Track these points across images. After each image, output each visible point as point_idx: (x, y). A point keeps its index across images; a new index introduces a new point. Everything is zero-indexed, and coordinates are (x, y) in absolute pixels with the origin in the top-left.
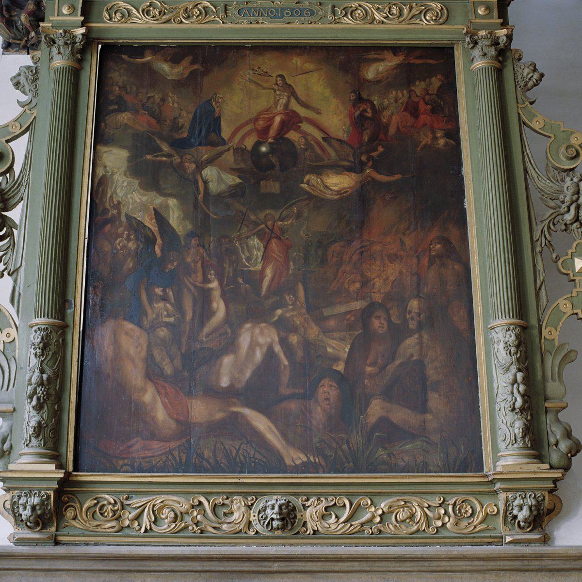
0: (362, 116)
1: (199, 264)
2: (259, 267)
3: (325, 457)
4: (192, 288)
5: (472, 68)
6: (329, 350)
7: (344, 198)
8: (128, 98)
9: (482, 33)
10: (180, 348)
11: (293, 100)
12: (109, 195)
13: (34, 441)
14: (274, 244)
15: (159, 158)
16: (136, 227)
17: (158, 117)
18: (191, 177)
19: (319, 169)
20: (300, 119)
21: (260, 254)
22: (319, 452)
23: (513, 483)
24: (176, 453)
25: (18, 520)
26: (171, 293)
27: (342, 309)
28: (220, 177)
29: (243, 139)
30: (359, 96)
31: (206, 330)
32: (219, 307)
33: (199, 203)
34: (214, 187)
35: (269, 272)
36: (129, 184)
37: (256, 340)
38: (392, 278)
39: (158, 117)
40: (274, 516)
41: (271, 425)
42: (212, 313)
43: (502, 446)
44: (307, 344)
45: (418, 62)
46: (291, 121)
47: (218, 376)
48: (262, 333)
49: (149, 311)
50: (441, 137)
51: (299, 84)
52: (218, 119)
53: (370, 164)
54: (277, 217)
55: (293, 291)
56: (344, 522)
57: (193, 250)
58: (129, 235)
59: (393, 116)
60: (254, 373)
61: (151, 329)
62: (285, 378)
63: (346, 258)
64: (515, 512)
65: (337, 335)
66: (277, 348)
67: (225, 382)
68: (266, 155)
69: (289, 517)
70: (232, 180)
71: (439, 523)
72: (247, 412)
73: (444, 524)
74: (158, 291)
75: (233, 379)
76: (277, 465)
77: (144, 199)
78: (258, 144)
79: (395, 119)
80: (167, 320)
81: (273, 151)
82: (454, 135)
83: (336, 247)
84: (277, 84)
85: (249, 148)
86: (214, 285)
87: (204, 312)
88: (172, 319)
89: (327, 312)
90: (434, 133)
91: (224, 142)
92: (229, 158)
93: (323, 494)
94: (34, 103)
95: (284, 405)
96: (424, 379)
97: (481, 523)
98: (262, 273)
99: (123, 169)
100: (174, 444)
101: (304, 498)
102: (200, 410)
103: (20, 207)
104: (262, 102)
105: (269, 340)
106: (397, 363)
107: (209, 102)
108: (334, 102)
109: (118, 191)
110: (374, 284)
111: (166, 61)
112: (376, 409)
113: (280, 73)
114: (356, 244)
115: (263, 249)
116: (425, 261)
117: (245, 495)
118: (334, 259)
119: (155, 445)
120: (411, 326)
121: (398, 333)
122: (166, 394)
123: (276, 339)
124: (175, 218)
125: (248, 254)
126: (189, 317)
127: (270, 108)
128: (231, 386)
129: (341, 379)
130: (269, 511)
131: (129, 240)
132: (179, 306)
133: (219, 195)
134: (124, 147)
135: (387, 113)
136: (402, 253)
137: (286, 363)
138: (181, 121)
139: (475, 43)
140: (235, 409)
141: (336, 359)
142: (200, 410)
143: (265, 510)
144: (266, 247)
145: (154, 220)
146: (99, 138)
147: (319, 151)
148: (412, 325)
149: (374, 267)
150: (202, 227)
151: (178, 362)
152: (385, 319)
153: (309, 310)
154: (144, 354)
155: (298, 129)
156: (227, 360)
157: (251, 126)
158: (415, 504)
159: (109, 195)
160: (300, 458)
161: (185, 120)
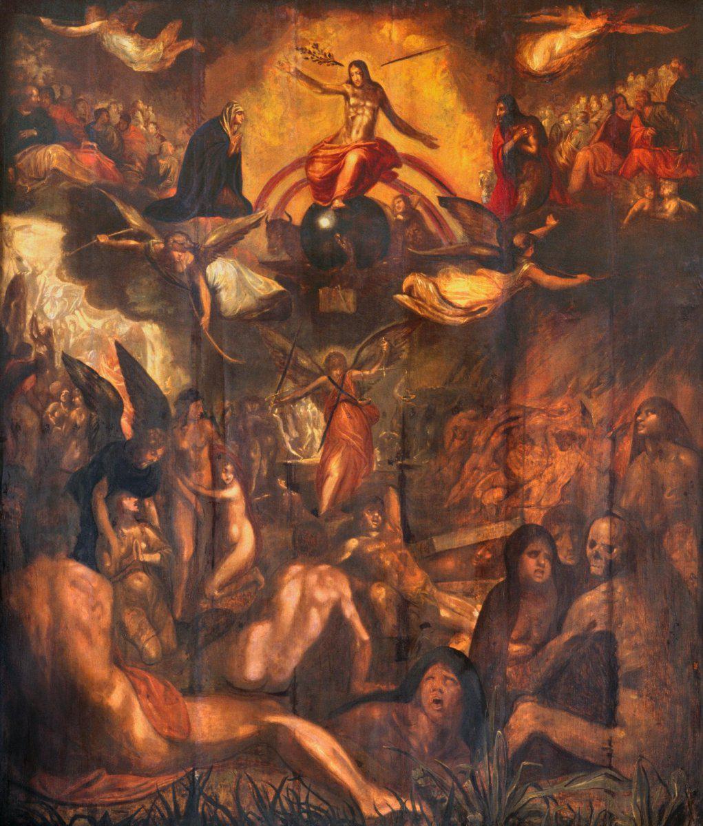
0: (518, 151)
1: (205, 454)
2: (316, 458)
3: (432, 803)
4: (192, 498)
6: (444, 613)
8: (57, 113)
10: (171, 610)
11: (382, 118)
12: (29, 317)
14: (344, 413)
15: (123, 242)
16: (87, 385)
17: (118, 152)
19: (429, 267)
20: (396, 160)
21: (318, 433)
26: (153, 509)
27: (470, 538)
28: (240, 280)
31: (220, 576)
32: (243, 533)
34: (231, 301)
36: (67, 293)
37: (311, 596)
38: (563, 480)
39: (118, 152)
41: (336, 746)
42: (232, 546)
44: (405, 605)
45: (635, 30)
46: (380, 162)
47: (243, 663)
48: (321, 582)
49: (114, 542)
50: (671, 197)
51: (393, 82)
52: (237, 158)
53: (530, 253)
54: (350, 360)
55: (380, 503)
57: (192, 426)
58: (71, 397)
59: (580, 155)
61: (117, 577)
62: (363, 665)
63: (479, 440)
65: (458, 585)
66: (350, 611)
67: (254, 670)
68: (329, 233)
70: (264, 285)
74: (130, 503)
75: (269, 667)
77: (98, 324)
78: (313, 213)
79: (583, 156)
80: (147, 558)
81: (339, 226)
83: (461, 420)
84: (350, 82)
85: (297, 220)
87: (216, 542)
88: (156, 557)
89: (440, 544)
90: (656, 188)
91: (247, 208)
92: (258, 240)
95: (359, 711)
96: (612, 666)
99: (54, 264)
100: (163, 781)
102: (209, 721)
104: (324, 124)
105: (334, 595)
106: (567, 636)
107: (216, 123)
108: (465, 121)
109: (47, 308)
110: (529, 490)
111: (129, 31)
112: (526, 718)
113: (357, 56)
114: (499, 414)
115: (323, 424)
116: (627, 446)
118: (457, 443)
120: (593, 569)
121: (570, 582)
122: (149, 695)
123: (348, 593)
125: (295, 434)
126: (187, 552)
127: (337, 135)
128: (267, 677)
129: (464, 665)
131: (71, 405)
132: (168, 534)
134: (54, 218)
135: (567, 145)
136: (583, 431)
137: (366, 637)
138: (163, 163)
140: (274, 719)
141: (456, 631)
142: (209, 721)
144: (329, 419)
145: (117, 368)
147: (431, 226)
148: (597, 568)
149: (530, 457)
151: (169, 635)
152: (547, 557)
153: (408, 537)
154: (106, 620)
155: (391, 180)
156: (259, 633)
157: (296, 176)
159: (29, 317)
161: (172, 159)
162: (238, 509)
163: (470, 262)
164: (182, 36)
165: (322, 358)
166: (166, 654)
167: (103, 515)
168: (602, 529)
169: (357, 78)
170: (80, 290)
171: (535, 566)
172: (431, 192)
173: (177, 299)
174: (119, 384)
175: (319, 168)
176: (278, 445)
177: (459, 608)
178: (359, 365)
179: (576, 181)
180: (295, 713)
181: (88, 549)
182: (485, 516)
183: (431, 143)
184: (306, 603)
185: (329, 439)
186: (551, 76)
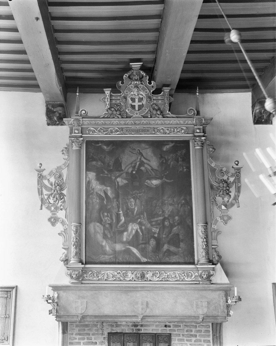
0: (162, 162)
2: (133, 207)
4: (115, 213)
6: (153, 231)
7: (157, 187)
8: (95, 157)
11: (142, 157)
12: (91, 186)
13: (75, 257)
14: (137, 201)
15: (104, 175)
16: (100, 196)
17: (103, 162)
18: (114, 181)
19: (150, 178)
20: (145, 163)
21: (134, 203)
22: (150, 258)
24: (112, 259)
25: (72, 277)
26: (109, 215)
27: (156, 219)
28: (122, 181)
29: (128, 169)
30: (161, 156)
31: (120, 225)
32: (123, 219)
33: (117, 189)
34: (120, 184)
35: (136, 209)
36: (96, 183)
37: (133, 228)
40: (139, 276)
41: (138, 251)
42: (121, 220)
45: (179, 145)
46: (142, 164)
47: (123, 238)
49: (103, 220)
50: (185, 169)
52: (121, 163)
53: (164, 177)
54: (138, 192)
56: (158, 278)
57: (115, 203)
60: (133, 237)
61: (104, 226)
63: (158, 205)
64: (203, 276)
65: (155, 226)
66: (139, 230)
67: (125, 239)
70: (125, 182)
71: (183, 278)
72: (132, 248)
73: (184, 278)
74: (106, 214)
75: (127, 239)
77: (101, 187)
78: (132, 171)
79: (172, 163)
80: (108, 222)
82: (189, 168)
84: (137, 152)
86: (121, 212)
88: (110, 222)
89: (152, 220)
90: (183, 167)
91: (122, 170)
92: (124, 175)
93: (152, 271)
94: (68, 159)
95: (140, 246)
97: (194, 278)
98: (134, 209)
100: (111, 256)
101: (147, 271)
102: (119, 247)
104: (134, 158)
105: (137, 228)
106: (172, 234)
108: (154, 158)
109: (93, 185)
110: (165, 212)
111: (105, 145)
112: (166, 247)
114: (161, 201)
115: (134, 202)
116: (180, 205)
118: (154, 205)
119: (106, 256)
120: (175, 224)
121: (172, 226)
122: (109, 243)
124: (109, 193)
125: (130, 204)
126: (114, 221)
127: (136, 160)
128: (127, 240)
130: (138, 275)
131: (97, 199)
132: (112, 219)
133: (122, 186)
134: (94, 172)
135: (170, 161)
136: (173, 203)
137: (141, 234)
142: (119, 247)
143: (137, 274)
144: (135, 202)
145: (104, 194)
146: (87, 169)
147: (150, 173)
149: (165, 207)
150: (117, 197)
152: (168, 222)
154: (102, 232)
155: (144, 166)
156: (125, 233)
158: (176, 273)
159: (91, 186)
161: (111, 163)
162: (122, 215)
163: (156, 178)
164: (113, 146)
166: (111, 237)
167: (102, 216)
168: (177, 218)
169: (138, 152)
170: (98, 182)
171: (166, 223)
174: (104, 196)
175: (133, 165)
176: (128, 205)
177: (156, 230)
178: (140, 193)
179: (171, 166)
180: (131, 246)
182: (159, 216)
183: (149, 161)
184: (132, 229)
186: (166, 151)
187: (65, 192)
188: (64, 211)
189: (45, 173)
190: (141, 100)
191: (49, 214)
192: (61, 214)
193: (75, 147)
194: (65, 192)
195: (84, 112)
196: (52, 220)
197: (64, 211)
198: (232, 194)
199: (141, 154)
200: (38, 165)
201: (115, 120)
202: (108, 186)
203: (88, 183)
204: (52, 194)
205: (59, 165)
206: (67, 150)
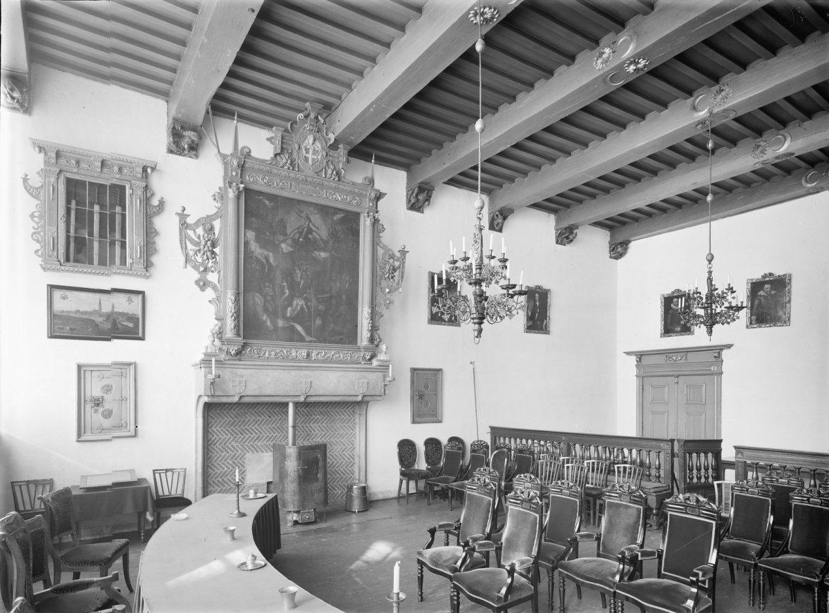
5: (365, 224)
9: (371, 214)
19: (320, 249)
20: (312, 231)
23: (366, 349)
29: (294, 235)
31: (283, 298)
32: (287, 292)
35: (302, 282)
37: (299, 303)
42: (285, 293)
43: (364, 339)
61: (265, 297)
67: (289, 315)
69: (308, 355)
70: (290, 249)
76: (302, 340)
78: (299, 238)
92: (289, 241)
103: (218, 248)
111: (268, 200)
117: (295, 348)
124: (271, 260)
128: (290, 316)
134: (253, 231)
139: (368, 216)
140: (293, 324)
142: (281, 323)
146: (246, 227)
156: (289, 309)
160: (310, 339)
163: (325, 250)
165: (300, 262)
167: (262, 285)
168: (344, 297)
172: (318, 237)
173: (275, 248)
181: (260, 291)
184: (297, 304)
185: (301, 278)
187: (217, 250)
188: (216, 274)
189: (190, 221)
190: (315, 152)
191: (196, 276)
192: (212, 277)
193: (231, 194)
194: (217, 250)
195: (248, 151)
196: (201, 283)
197: (216, 274)
198: (396, 278)
199: (308, 218)
200: (181, 209)
201: (284, 171)
202: (270, 251)
203: (246, 243)
204: (199, 250)
205: (210, 214)
206: (221, 196)
